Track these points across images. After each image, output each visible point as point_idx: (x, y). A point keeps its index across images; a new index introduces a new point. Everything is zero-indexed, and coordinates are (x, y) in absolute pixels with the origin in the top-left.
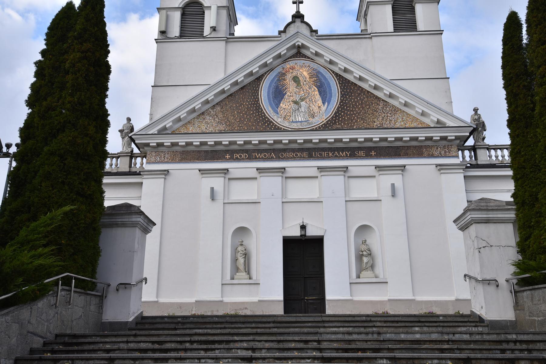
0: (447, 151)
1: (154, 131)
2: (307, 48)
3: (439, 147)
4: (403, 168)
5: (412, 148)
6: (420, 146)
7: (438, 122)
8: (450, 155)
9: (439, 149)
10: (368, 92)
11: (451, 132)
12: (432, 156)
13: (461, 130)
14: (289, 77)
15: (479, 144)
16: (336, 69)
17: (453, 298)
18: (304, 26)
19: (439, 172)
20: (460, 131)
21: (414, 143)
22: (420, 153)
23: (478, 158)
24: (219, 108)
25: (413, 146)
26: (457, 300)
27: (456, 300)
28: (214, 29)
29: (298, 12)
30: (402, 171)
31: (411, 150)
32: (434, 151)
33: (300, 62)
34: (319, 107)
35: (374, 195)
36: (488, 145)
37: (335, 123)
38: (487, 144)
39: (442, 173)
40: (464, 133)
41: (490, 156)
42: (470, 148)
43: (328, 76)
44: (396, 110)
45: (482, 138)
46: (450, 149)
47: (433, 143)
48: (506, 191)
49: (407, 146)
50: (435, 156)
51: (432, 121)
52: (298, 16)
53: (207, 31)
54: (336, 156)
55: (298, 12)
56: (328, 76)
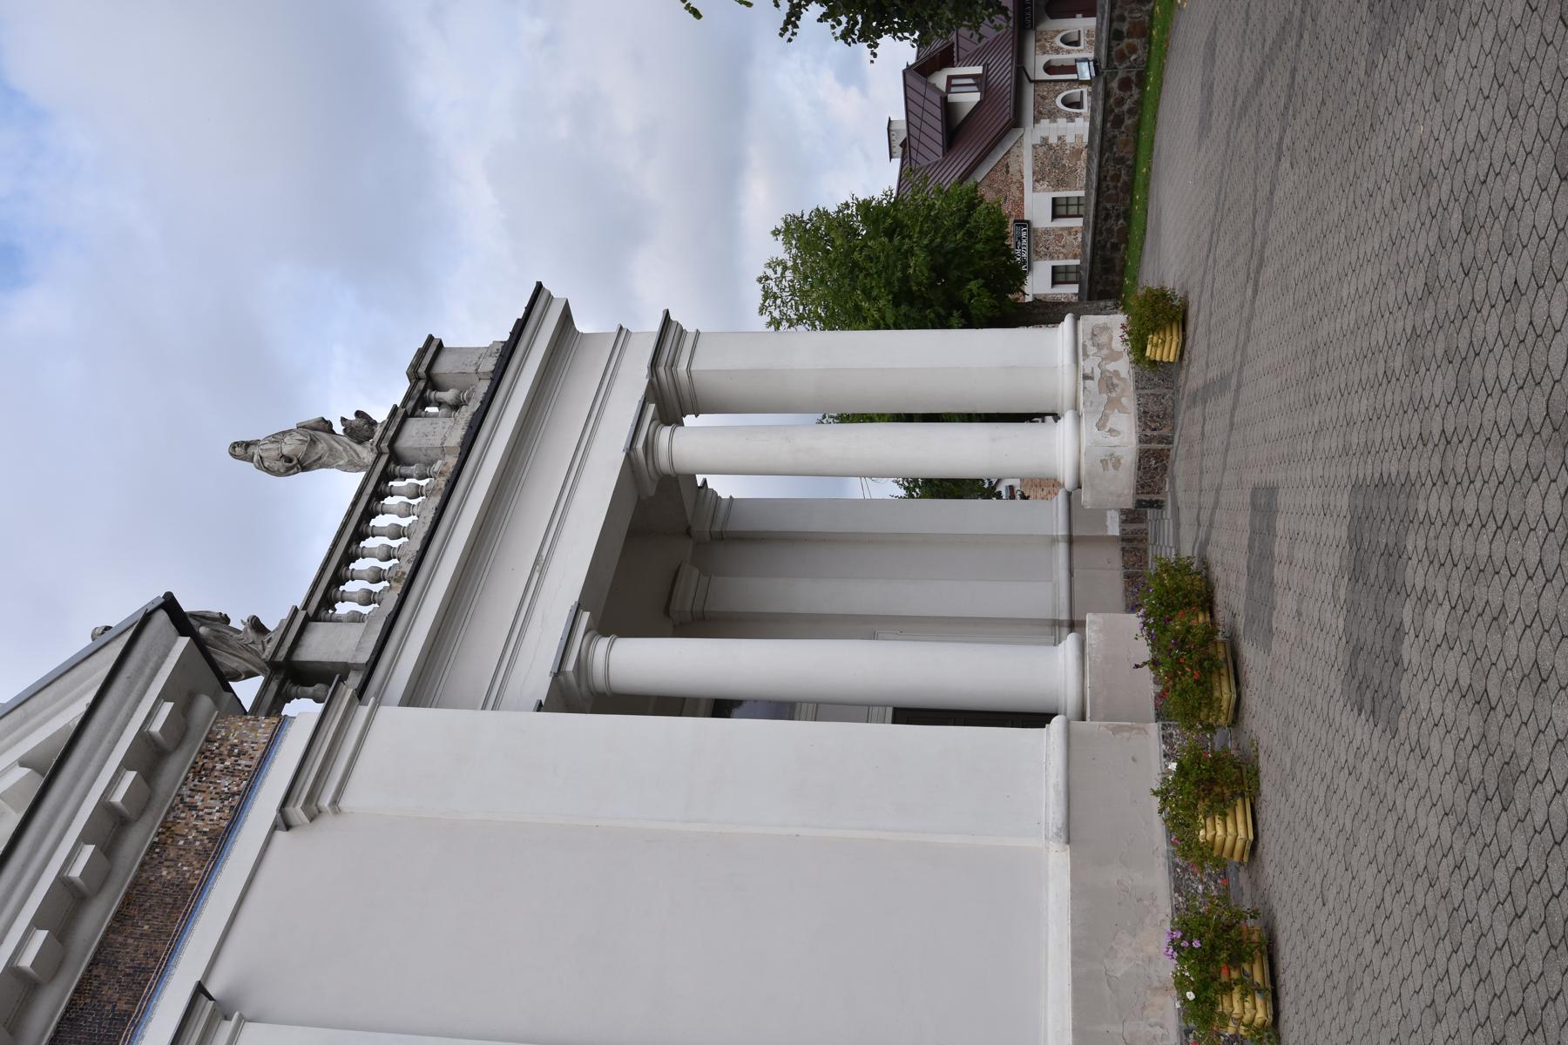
0: (227, 763)
3: (188, 800)
5: (120, 939)
6: (127, 894)
8: (258, 754)
9: (198, 797)
11: (126, 709)
12: (220, 841)
13: (145, 661)
15: (270, 648)
17: (1058, 860)
19: (326, 821)
20: (147, 671)
21: (94, 922)
22: (168, 900)
23: (341, 659)
25: (110, 929)
26: (1069, 833)
27: (1068, 841)
30: (222, 1012)
31: (125, 945)
32: (200, 823)
36: (296, 611)
38: (285, 614)
39: (335, 802)
40: (165, 656)
41: (356, 618)
42: (274, 686)
45: (252, 635)
46: (224, 750)
47: (148, 818)
48: (536, 575)
49: (94, 962)
50: (225, 824)
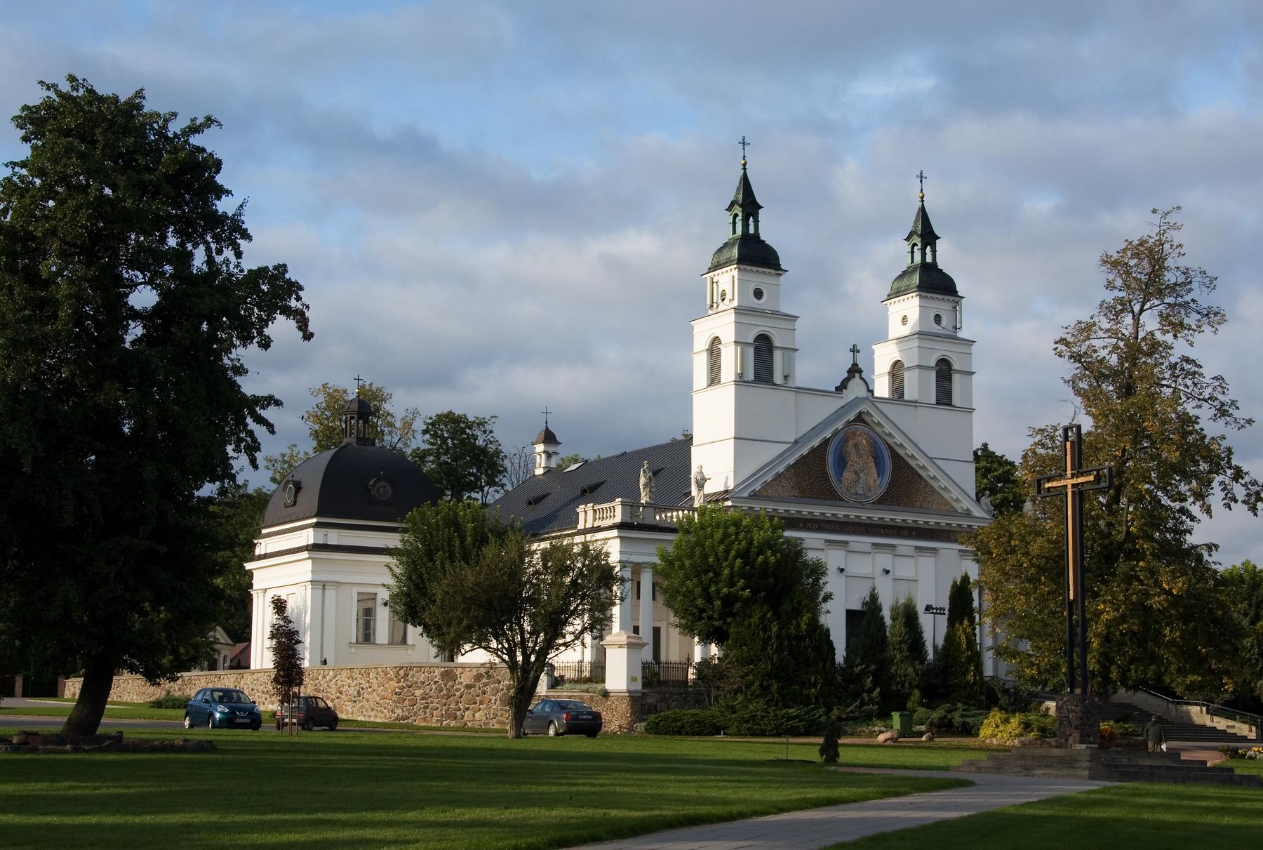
1: (745, 494)
2: (871, 416)
4: (935, 550)
7: (968, 509)
10: (914, 469)
12: (955, 541)
14: (851, 443)
16: (890, 441)
18: (862, 381)
24: (793, 471)
28: (786, 377)
29: (855, 365)
33: (860, 428)
34: (875, 481)
35: (911, 575)
37: (886, 500)
43: (883, 447)
44: (933, 491)
51: (962, 508)
52: (855, 370)
53: (778, 378)
54: (886, 534)
55: (855, 365)
56: (883, 447)
